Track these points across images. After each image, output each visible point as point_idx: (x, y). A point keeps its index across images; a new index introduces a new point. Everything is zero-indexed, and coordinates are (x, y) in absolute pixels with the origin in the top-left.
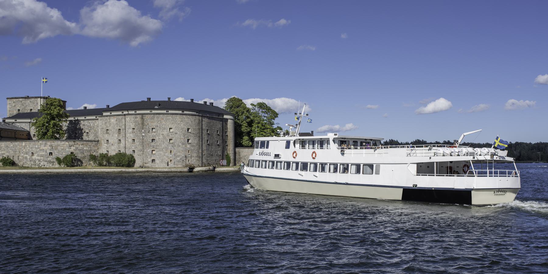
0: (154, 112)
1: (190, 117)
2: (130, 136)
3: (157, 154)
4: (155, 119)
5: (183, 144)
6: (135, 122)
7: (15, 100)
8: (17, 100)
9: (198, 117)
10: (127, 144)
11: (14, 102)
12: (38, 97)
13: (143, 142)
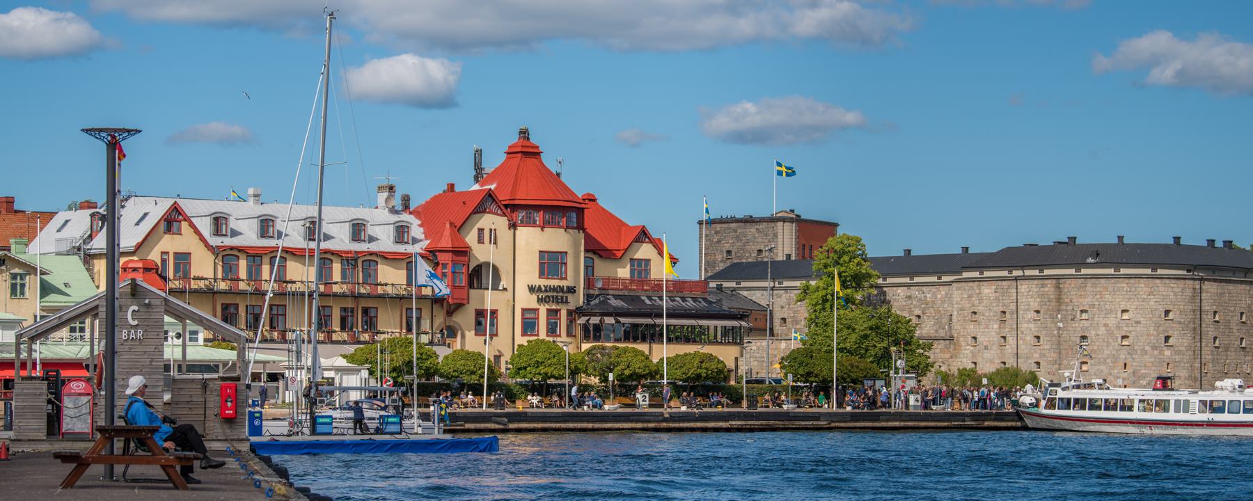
0: (1084, 271)
1: (1173, 283)
2: (1029, 328)
3: (1092, 371)
4: (1089, 288)
5: (1154, 348)
7: (718, 227)
8: (725, 225)
9: (1190, 282)
10: (1022, 347)
11: (717, 232)
13: (1059, 344)
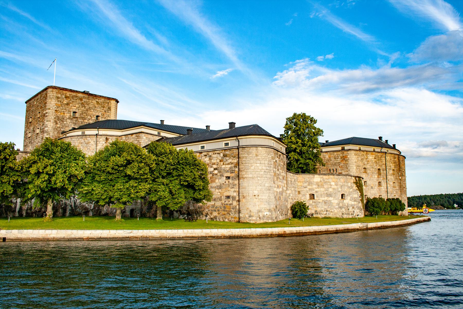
6: (395, 162)
7: (68, 94)
10: (389, 188)
11: (66, 97)
12: (113, 99)
